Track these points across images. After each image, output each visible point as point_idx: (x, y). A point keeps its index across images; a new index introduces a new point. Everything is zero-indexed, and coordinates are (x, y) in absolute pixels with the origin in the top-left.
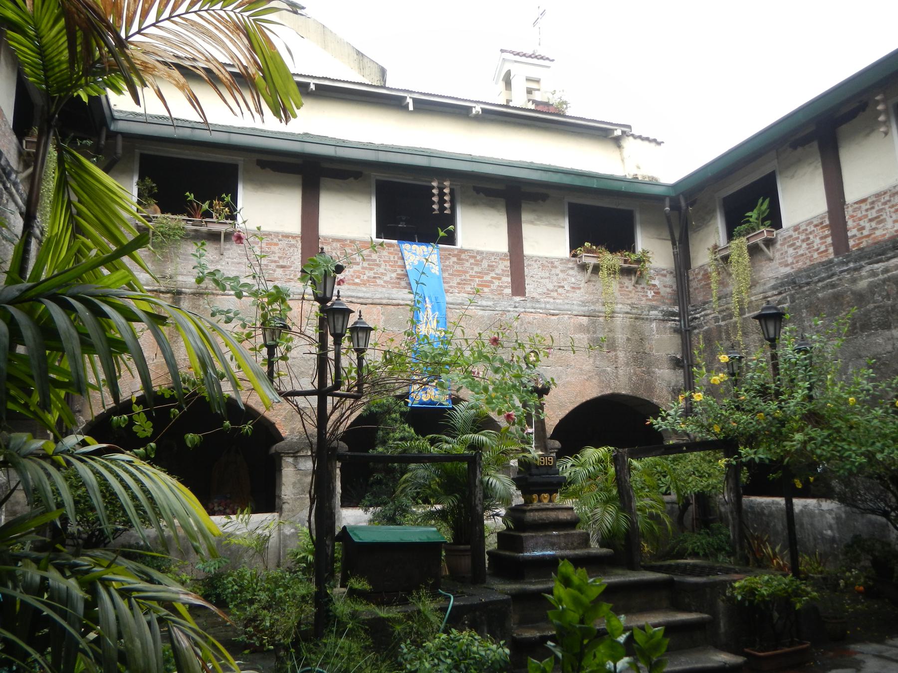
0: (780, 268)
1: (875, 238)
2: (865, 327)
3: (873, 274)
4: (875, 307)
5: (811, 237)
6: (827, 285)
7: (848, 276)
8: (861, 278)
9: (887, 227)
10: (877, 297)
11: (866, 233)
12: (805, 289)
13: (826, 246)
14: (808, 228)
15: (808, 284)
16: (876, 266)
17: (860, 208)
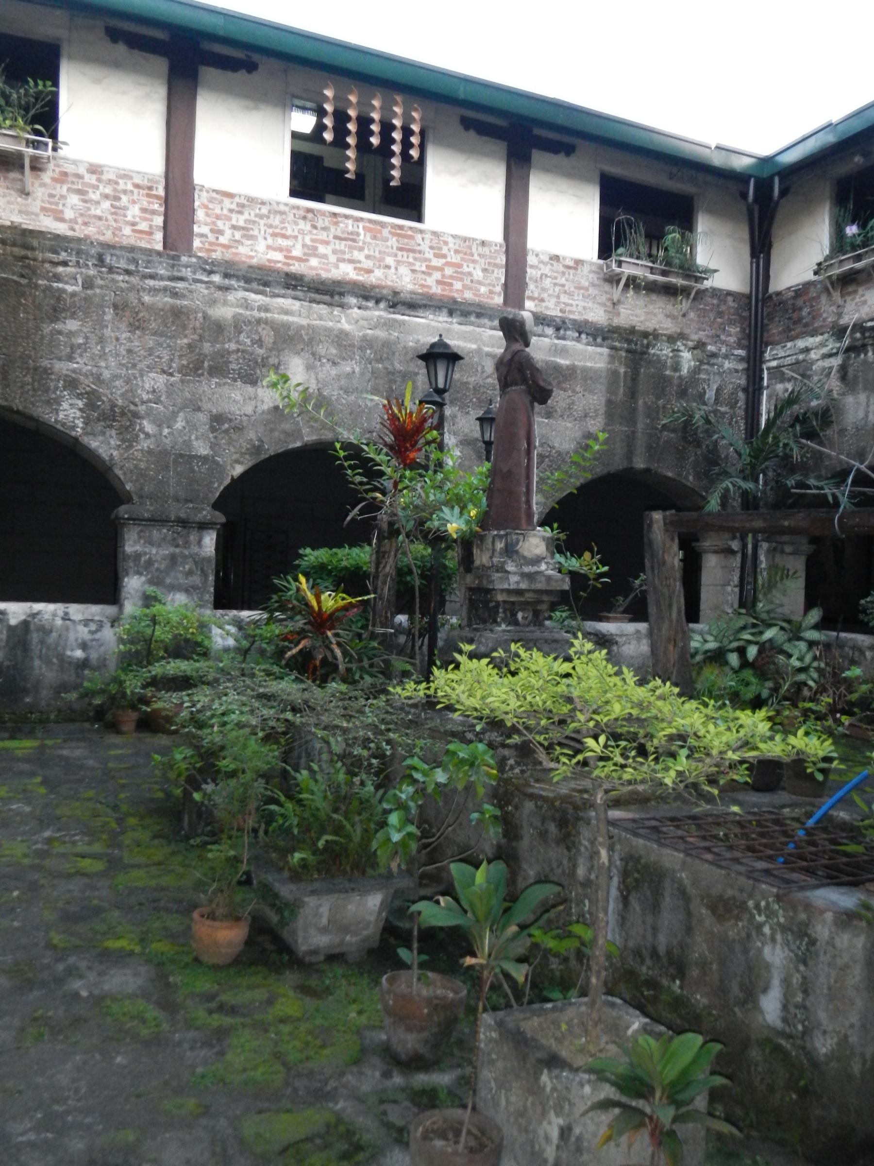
0: (42, 217)
1: (236, 254)
2: (219, 369)
3: (247, 305)
4: (238, 350)
5: (124, 199)
6: (165, 289)
7: (206, 292)
8: (225, 303)
9: (257, 248)
10: (242, 337)
11: (223, 240)
12: (121, 278)
13: (151, 227)
14: (121, 181)
15: (128, 272)
16: (253, 296)
17: (221, 202)
